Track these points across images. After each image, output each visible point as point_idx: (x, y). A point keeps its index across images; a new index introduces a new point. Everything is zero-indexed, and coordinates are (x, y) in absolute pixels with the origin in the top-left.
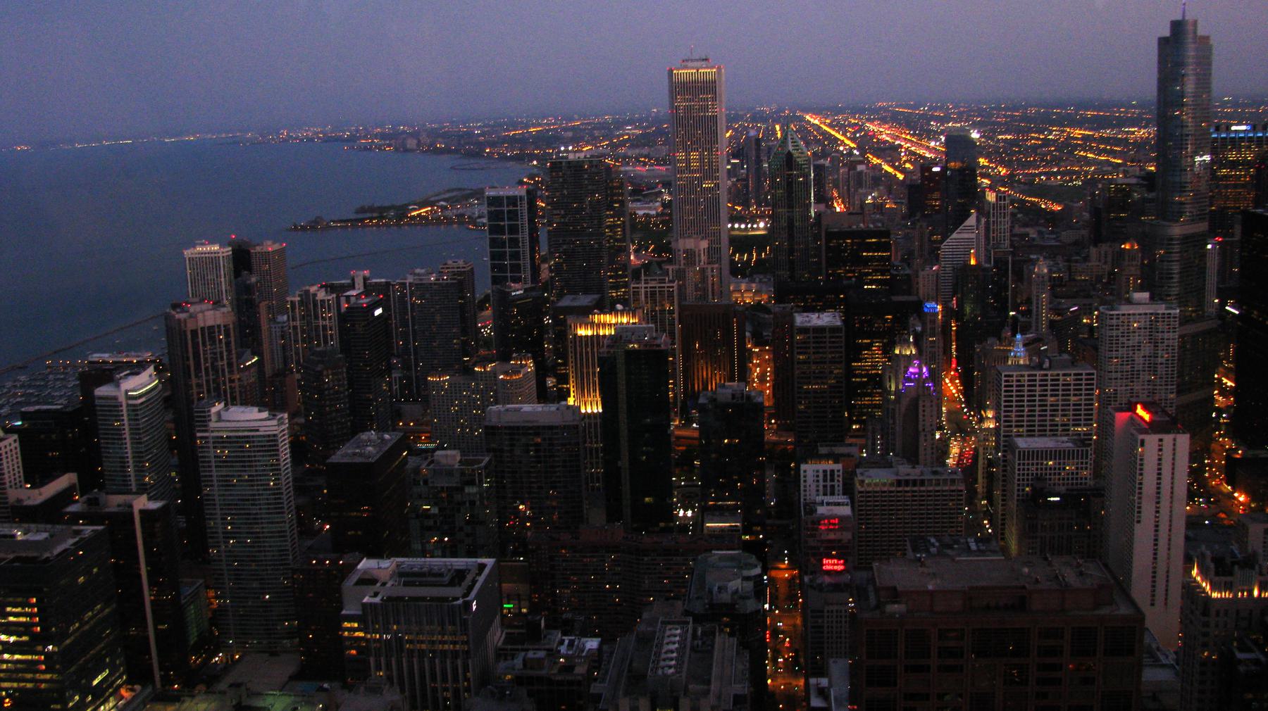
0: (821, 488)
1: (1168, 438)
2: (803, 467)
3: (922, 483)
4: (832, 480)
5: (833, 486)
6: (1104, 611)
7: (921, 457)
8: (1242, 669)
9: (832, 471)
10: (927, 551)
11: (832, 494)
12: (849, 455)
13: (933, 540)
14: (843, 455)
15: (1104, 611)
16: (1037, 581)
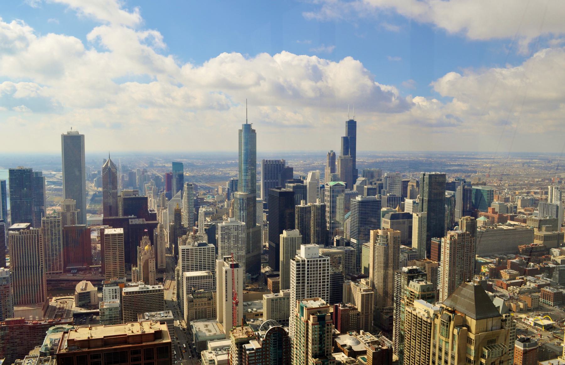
0: (111, 297)
1: (235, 270)
2: (104, 288)
3: (148, 291)
4: (116, 293)
5: (116, 295)
6: (157, 342)
7: (150, 281)
8: (248, 352)
9: (116, 289)
10: (144, 318)
11: (116, 298)
12: (122, 283)
13: (147, 313)
14: (119, 283)
15: (157, 342)
16: (133, 332)
